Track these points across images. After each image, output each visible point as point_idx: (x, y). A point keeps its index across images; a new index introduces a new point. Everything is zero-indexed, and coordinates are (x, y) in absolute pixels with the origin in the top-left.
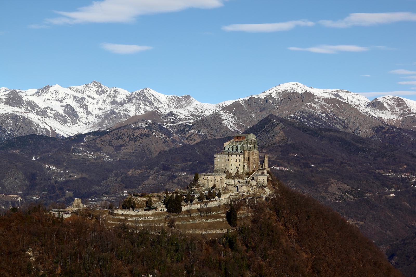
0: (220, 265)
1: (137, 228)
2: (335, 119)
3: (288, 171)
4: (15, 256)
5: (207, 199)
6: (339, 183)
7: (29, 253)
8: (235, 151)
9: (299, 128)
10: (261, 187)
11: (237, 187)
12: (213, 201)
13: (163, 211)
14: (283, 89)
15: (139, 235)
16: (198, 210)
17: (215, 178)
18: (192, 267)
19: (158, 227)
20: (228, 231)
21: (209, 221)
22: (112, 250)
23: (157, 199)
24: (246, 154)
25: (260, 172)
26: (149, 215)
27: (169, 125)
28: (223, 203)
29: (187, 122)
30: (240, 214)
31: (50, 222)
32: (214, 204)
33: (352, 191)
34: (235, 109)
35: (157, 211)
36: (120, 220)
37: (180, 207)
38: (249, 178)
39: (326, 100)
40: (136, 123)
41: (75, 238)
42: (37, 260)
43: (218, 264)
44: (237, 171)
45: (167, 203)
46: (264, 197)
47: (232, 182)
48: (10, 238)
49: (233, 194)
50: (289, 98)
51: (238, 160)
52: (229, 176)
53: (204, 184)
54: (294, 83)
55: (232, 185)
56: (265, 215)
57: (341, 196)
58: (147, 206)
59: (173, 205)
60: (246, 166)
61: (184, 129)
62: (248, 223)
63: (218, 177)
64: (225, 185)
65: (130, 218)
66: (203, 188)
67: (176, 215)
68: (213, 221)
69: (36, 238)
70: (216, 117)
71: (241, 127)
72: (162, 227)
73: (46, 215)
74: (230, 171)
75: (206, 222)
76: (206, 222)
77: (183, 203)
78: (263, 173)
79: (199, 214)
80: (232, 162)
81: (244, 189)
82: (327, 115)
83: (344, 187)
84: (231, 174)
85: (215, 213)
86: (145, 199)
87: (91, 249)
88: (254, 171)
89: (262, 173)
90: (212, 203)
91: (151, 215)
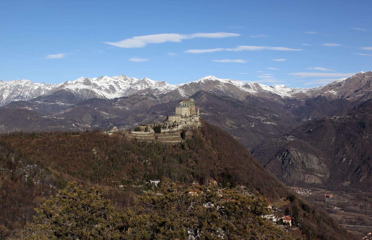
0: (178, 156)
1: (141, 139)
2: (229, 92)
3: (208, 115)
4: (88, 151)
6: (231, 120)
7: (94, 150)
8: (185, 106)
9: (213, 96)
10: (196, 122)
11: (186, 122)
12: (175, 128)
14: (206, 79)
15: (142, 143)
16: (168, 132)
18: (165, 157)
19: (151, 139)
20: (181, 141)
22: (130, 149)
23: (150, 127)
24: (190, 107)
26: (146, 134)
27: (156, 94)
30: (187, 134)
31: (103, 137)
32: (175, 129)
33: (236, 124)
34: (185, 87)
36: (134, 136)
37: (160, 130)
39: (225, 84)
40: (141, 93)
41: (114, 144)
42: (97, 153)
43: (177, 156)
44: (186, 115)
45: (154, 129)
47: (183, 120)
48: (85, 144)
49: (184, 125)
50: (208, 82)
52: (182, 117)
53: (171, 121)
54: (211, 76)
55: (183, 121)
56: (198, 134)
57: (231, 126)
58: (146, 130)
59: (157, 130)
60: (190, 113)
61: (162, 96)
62: (190, 138)
63: (177, 118)
64: (180, 121)
65: (138, 135)
69: (97, 144)
70: (176, 91)
71: (188, 95)
72: (152, 139)
73: (101, 134)
74: (182, 115)
77: (162, 129)
78: (197, 116)
79: (169, 134)
80: (183, 111)
81: (189, 123)
82: (225, 90)
83: (233, 122)
85: (176, 133)
86: (145, 127)
87: (121, 149)
91: (148, 134)
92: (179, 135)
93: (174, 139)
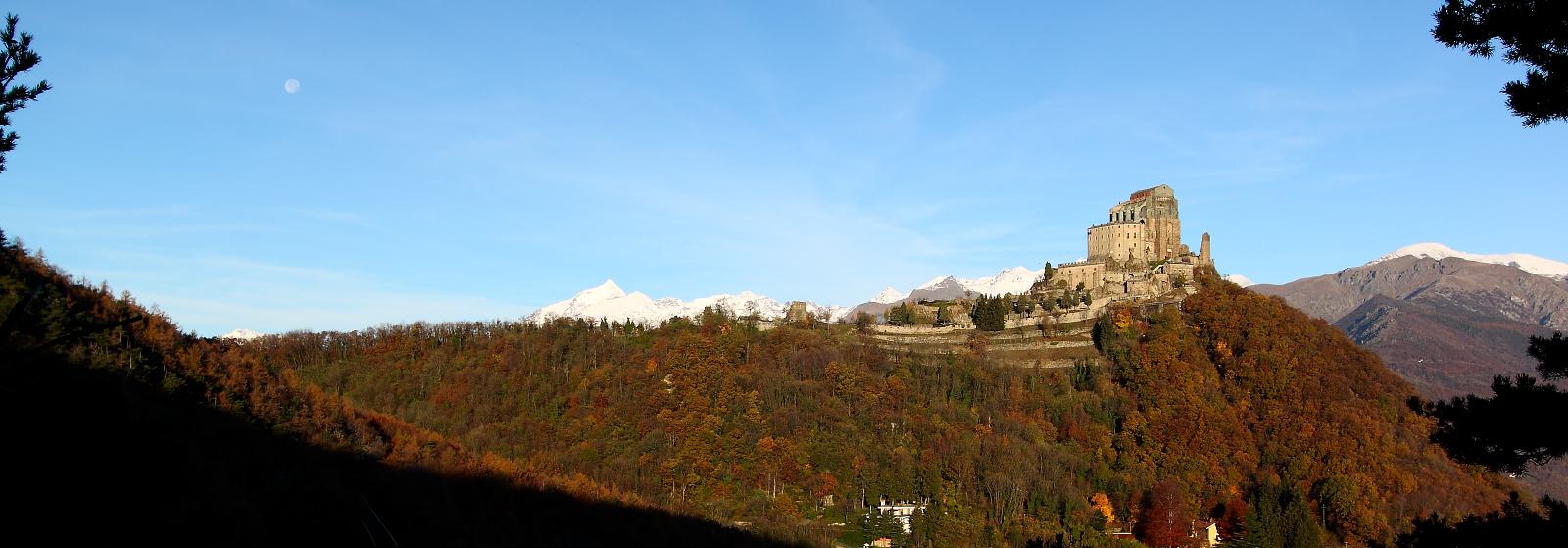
5: (1062, 307)
10: (1178, 283)
11: (1125, 285)
12: (1075, 311)
13: (969, 327)
16: (1040, 327)
21: (1058, 346)
25: (1179, 260)
28: (1090, 315)
32: (1073, 317)
35: (957, 327)
47: (1119, 277)
51: (1131, 236)
53: (1063, 284)
60: (1152, 249)
63: (1089, 269)
64: (1102, 284)
67: (992, 336)
68: (1068, 346)
74: (1116, 257)
75: (1053, 347)
76: (1053, 347)
80: (1120, 240)
85: (1072, 333)
91: (943, 335)
92: (1087, 340)
93: (1058, 355)
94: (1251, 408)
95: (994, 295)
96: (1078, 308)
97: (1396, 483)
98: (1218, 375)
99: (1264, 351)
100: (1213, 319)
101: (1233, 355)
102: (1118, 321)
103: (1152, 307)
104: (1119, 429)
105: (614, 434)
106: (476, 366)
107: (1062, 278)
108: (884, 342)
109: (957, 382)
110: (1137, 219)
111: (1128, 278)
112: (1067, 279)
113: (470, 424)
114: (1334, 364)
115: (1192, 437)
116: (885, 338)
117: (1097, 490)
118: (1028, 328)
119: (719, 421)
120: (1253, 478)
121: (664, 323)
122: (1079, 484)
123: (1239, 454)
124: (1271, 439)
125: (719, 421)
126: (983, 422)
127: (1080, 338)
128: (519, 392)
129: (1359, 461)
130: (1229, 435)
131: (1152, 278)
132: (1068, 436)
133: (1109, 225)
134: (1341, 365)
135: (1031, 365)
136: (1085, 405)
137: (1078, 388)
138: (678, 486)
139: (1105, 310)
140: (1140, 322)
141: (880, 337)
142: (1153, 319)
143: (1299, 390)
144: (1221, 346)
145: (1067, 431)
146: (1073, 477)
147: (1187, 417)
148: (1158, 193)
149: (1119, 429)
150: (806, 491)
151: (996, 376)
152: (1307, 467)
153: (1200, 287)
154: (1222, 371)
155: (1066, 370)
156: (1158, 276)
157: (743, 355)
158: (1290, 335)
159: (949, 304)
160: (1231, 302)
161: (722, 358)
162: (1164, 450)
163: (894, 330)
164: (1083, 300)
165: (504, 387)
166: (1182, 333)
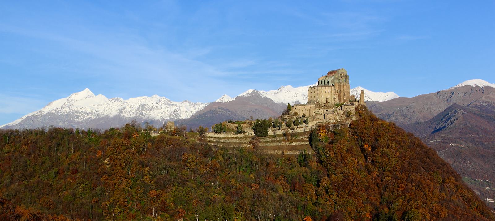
5: (295, 125)
11: (324, 115)
16: (284, 135)
17: (305, 108)
21: (292, 144)
23: (248, 125)
25: (349, 103)
26: (236, 138)
29: (388, 112)
32: (300, 130)
35: (246, 134)
38: (338, 108)
46: (349, 124)
47: (322, 111)
51: (327, 92)
53: (296, 114)
55: (321, 114)
60: (337, 98)
63: (308, 107)
64: (314, 114)
66: (294, 117)
67: (263, 138)
68: (297, 144)
76: (290, 144)
79: (284, 138)
80: (322, 94)
84: (321, 105)
85: (300, 138)
88: (344, 102)
89: (351, 104)
90: (298, 129)
91: (239, 138)
94: (378, 176)
95: (264, 119)
96: (302, 126)
97: (438, 213)
98: (364, 160)
99: (385, 149)
100: (363, 133)
101: (371, 150)
102: (320, 132)
103: (335, 126)
104: (318, 186)
105: (81, 187)
106: (15, 151)
107: (295, 111)
108: (211, 142)
109: (245, 163)
110: (330, 84)
111: (325, 112)
112: (297, 111)
113: (12, 182)
114: (415, 155)
115: (351, 190)
116: (211, 139)
117: (307, 215)
118: (279, 135)
119: (131, 182)
120: (377, 209)
121: (106, 131)
122: (298, 212)
123: (371, 198)
124: (386, 191)
125: (131, 182)
126: (255, 182)
127: (302, 140)
128: (35, 165)
129: (423, 202)
130: (367, 189)
131: (336, 112)
132: (294, 189)
133: (318, 86)
134: (418, 156)
135: (280, 153)
136: (303, 174)
137: (301, 166)
138: (110, 214)
139: (314, 127)
140: (330, 133)
141: (209, 139)
142: (336, 132)
143: (399, 168)
144: (366, 146)
145: (294, 186)
146: (296, 209)
147: (349, 180)
148: (340, 72)
149: (318, 186)
150: (171, 216)
151: (262, 159)
152: (400, 205)
153: (359, 117)
154: (366, 157)
155: (296, 156)
156: (339, 111)
157: (144, 149)
158: (397, 141)
159: (243, 123)
160: (371, 124)
161: (133, 150)
162: (338, 196)
163: (216, 135)
164: (305, 122)
165: (28, 163)
166: (349, 139)
